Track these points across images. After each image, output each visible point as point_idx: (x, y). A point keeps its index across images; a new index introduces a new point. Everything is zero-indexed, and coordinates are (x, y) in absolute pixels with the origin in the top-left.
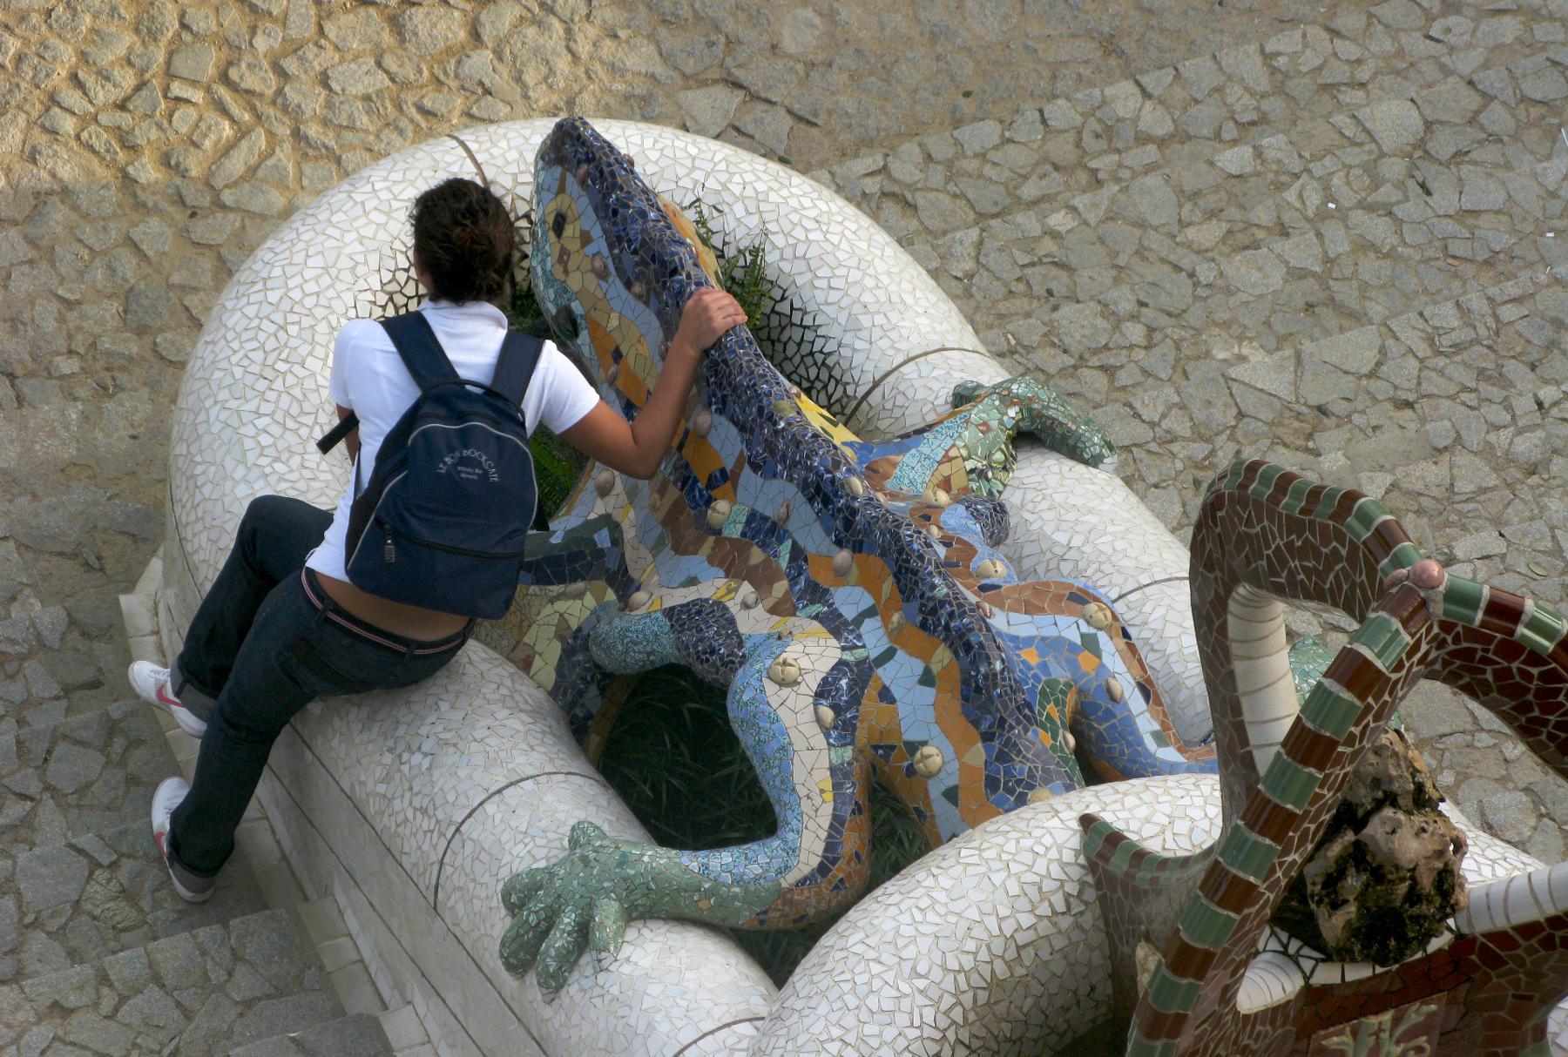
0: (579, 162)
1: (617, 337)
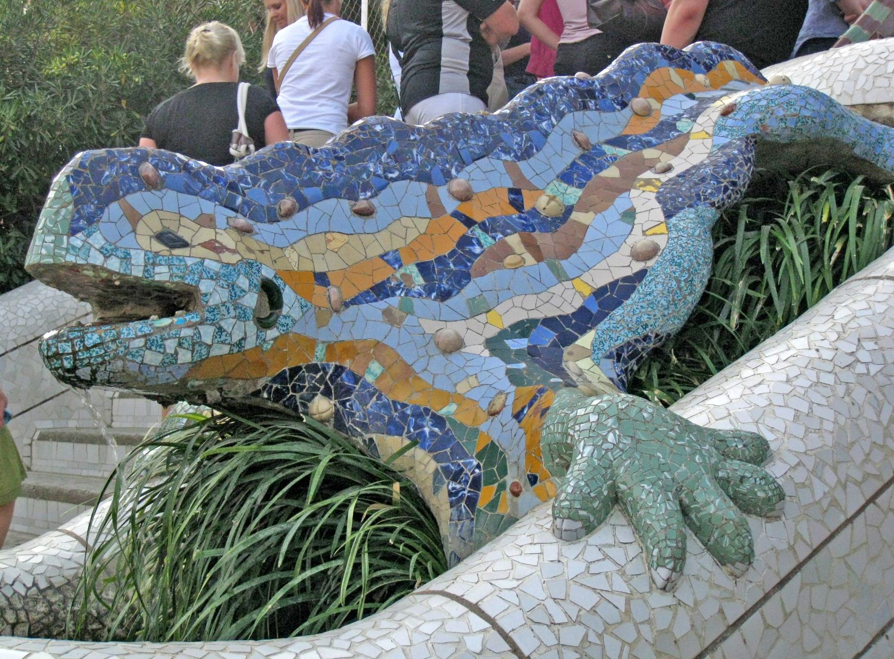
0: (135, 170)
1: (307, 267)
